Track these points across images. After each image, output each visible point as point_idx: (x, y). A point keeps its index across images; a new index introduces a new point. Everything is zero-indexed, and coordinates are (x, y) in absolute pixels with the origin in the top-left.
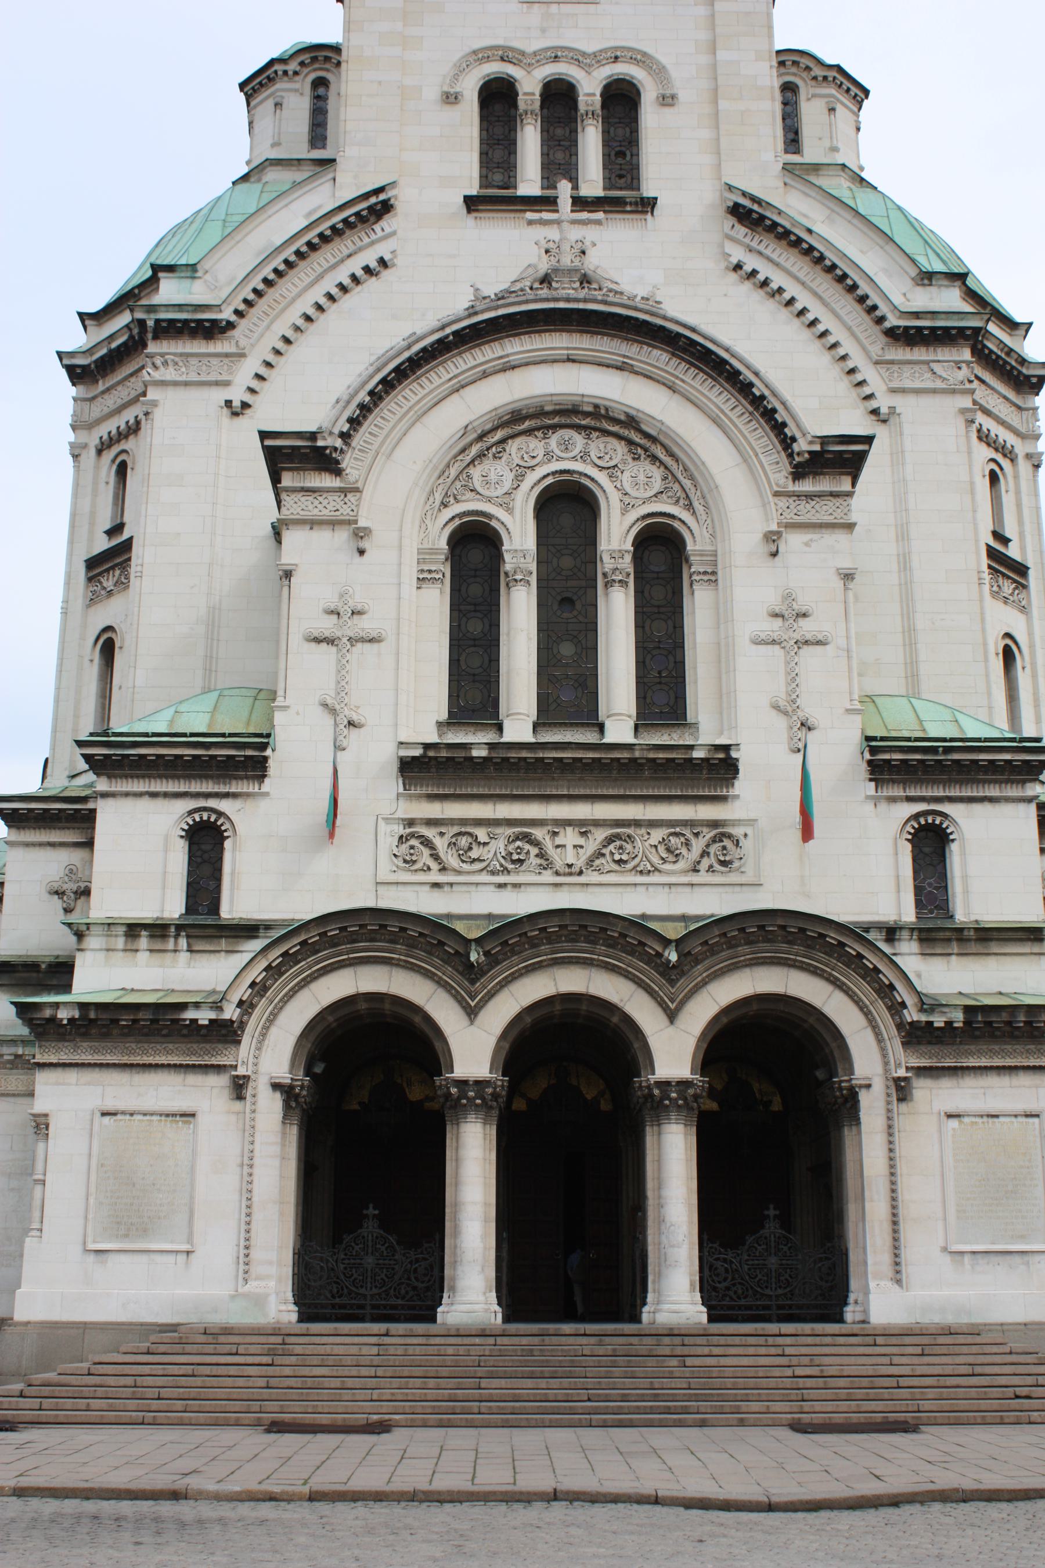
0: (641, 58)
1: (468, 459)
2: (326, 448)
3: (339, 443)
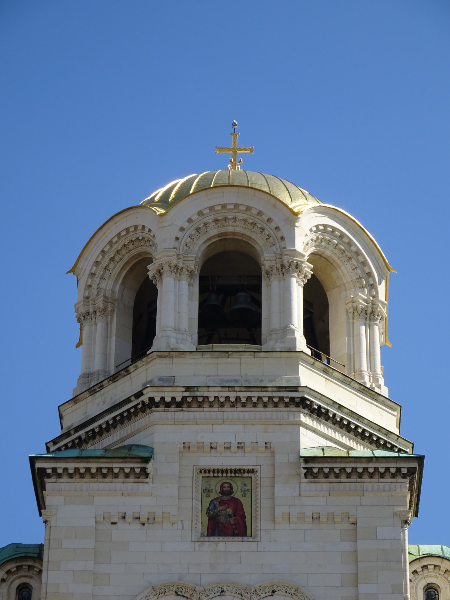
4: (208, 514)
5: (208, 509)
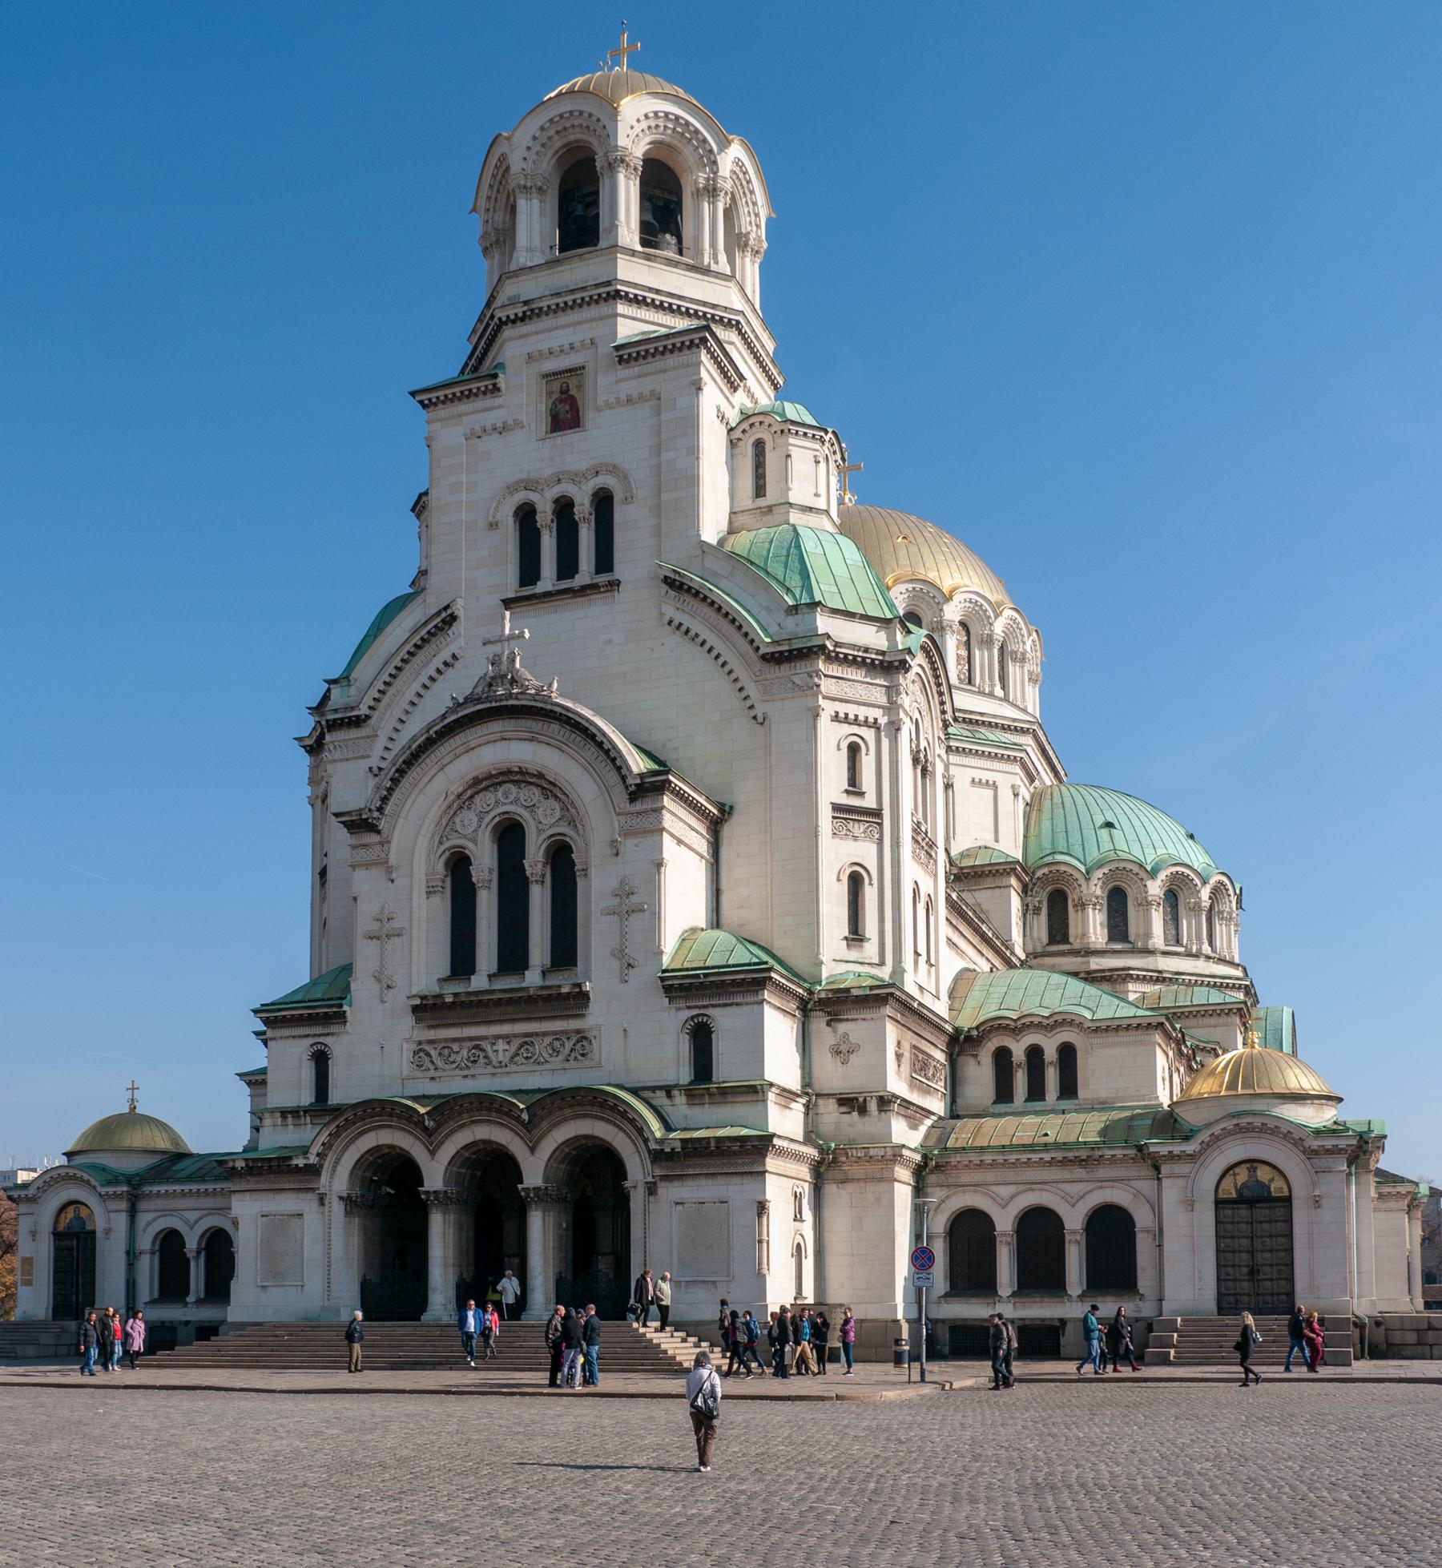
0: (614, 469)
1: (452, 812)
2: (368, 819)
3: (376, 814)
5: (551, 410)
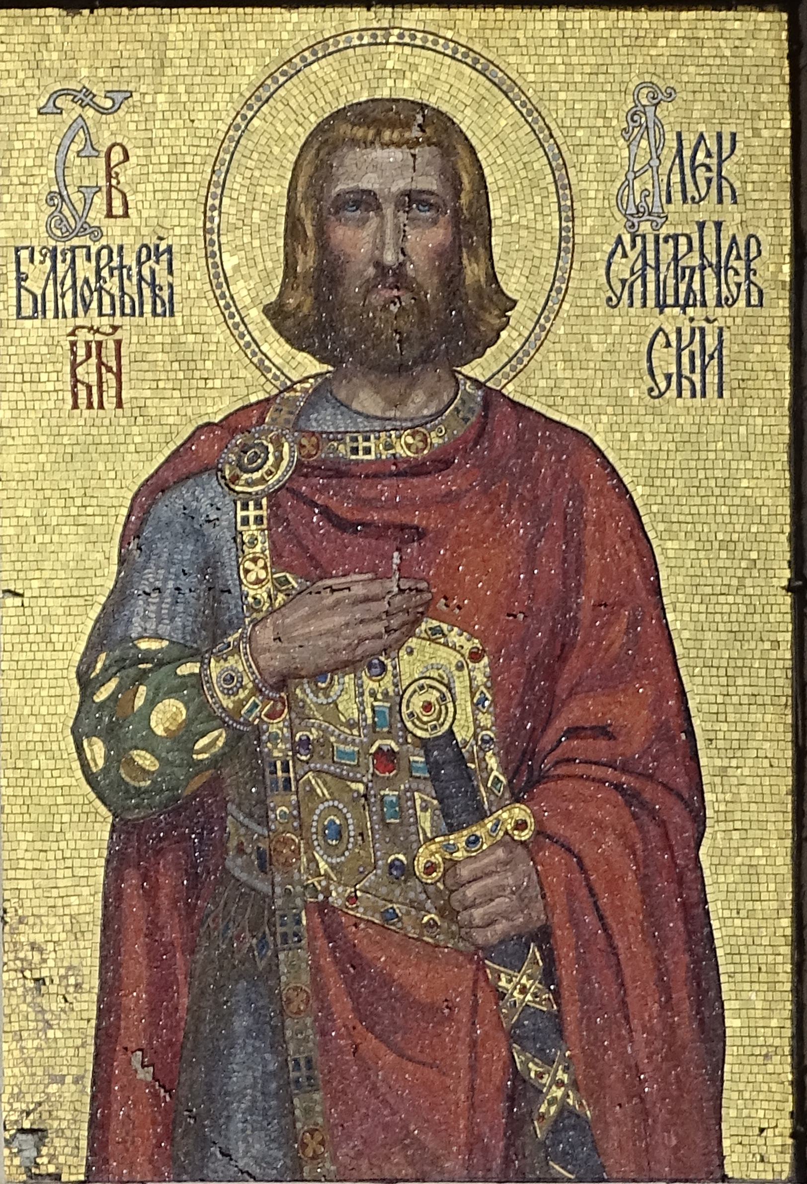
4: (97, 751)
